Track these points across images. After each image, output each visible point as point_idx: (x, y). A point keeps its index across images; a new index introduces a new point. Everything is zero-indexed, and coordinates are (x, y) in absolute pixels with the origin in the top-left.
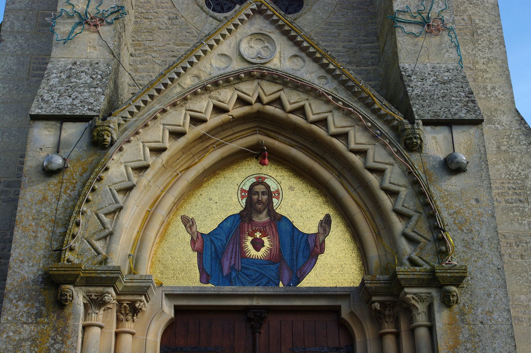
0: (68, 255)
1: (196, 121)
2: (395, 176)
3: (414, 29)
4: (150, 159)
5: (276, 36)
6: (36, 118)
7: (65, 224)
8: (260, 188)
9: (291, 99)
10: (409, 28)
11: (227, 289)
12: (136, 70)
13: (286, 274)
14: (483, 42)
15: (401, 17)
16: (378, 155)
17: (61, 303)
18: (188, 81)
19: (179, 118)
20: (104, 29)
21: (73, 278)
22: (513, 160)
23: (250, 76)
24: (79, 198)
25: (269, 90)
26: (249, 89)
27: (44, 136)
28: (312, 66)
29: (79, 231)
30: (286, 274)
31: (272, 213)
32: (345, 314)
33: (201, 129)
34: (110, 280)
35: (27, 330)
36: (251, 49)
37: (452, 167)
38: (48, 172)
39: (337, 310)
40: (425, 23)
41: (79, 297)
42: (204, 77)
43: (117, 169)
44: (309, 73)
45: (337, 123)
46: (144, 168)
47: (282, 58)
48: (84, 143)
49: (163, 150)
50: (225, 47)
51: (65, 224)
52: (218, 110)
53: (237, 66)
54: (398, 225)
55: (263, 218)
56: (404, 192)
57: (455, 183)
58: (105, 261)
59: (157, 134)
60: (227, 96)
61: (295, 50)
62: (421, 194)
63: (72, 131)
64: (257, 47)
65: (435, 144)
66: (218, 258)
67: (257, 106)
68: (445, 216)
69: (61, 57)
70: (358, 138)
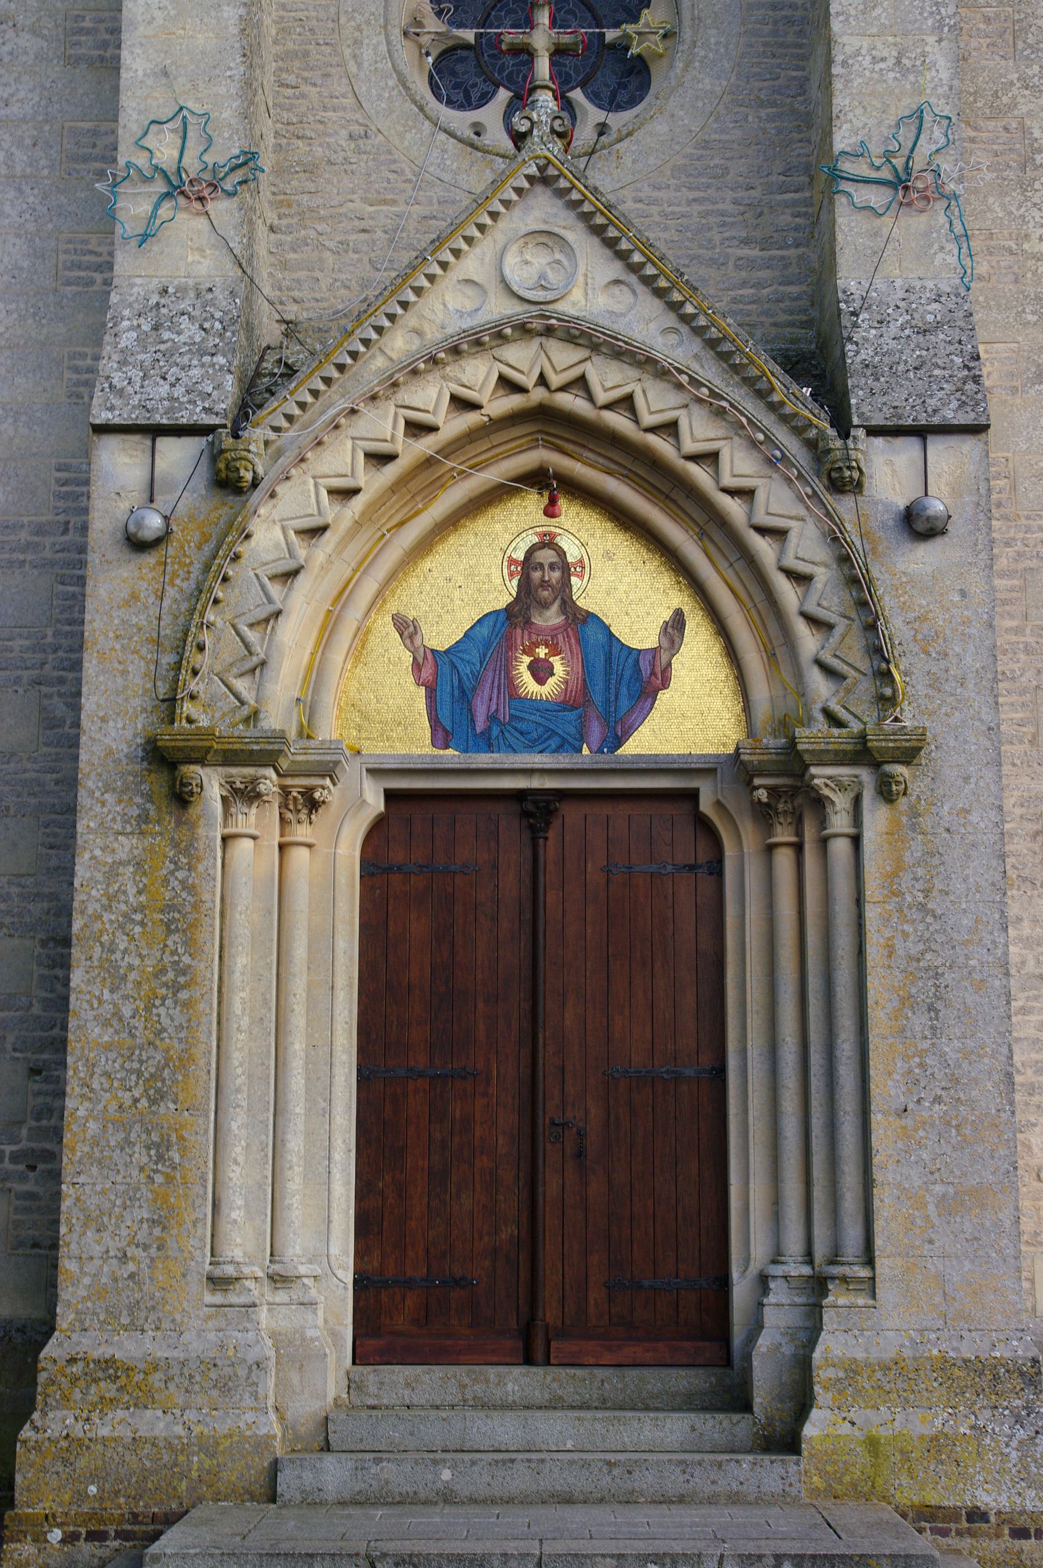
1: (417, 429)
2: (807, 546)
5: (576, 235)
7: (178, 652)
9: (608, 378)
11: (483, 759)
13: (596, 731)
16: (776, 501)
18: (400, 344)
19: (383, 425)
20: (220, 208)
23: (524, 330)
24: (201, 597)
25: (563, 359)
26: (522, 358)
27: (120, 465)
28: (650, 306)
30: (596, 731)
31: (568, 605)
33: (427, 445)
36: (526, 267)
37: (918, 525)
38: (137, 545)
42: (433, 335)
43: (268, 535)
44: (643, 322)
45: (699, 431)
46: (317, 532)
47: (592, 290)
50: (474, 264)
51: (178, 652)
52: (461, 404)
53: (499, 308)
54: (808, 641)
55: (551, 618)
56: (823, 576)
57: (922, 558)
59: (341, 459)
60: (477, 375)
61: (615, 269)
62: (856, 582)
63: (177, 456)
64: (539, 260)
65: (890, 473)
66: (464, 696)
67: (538, 395)
68: (896, 625)
69: (136, 276)
70: (739, 464)
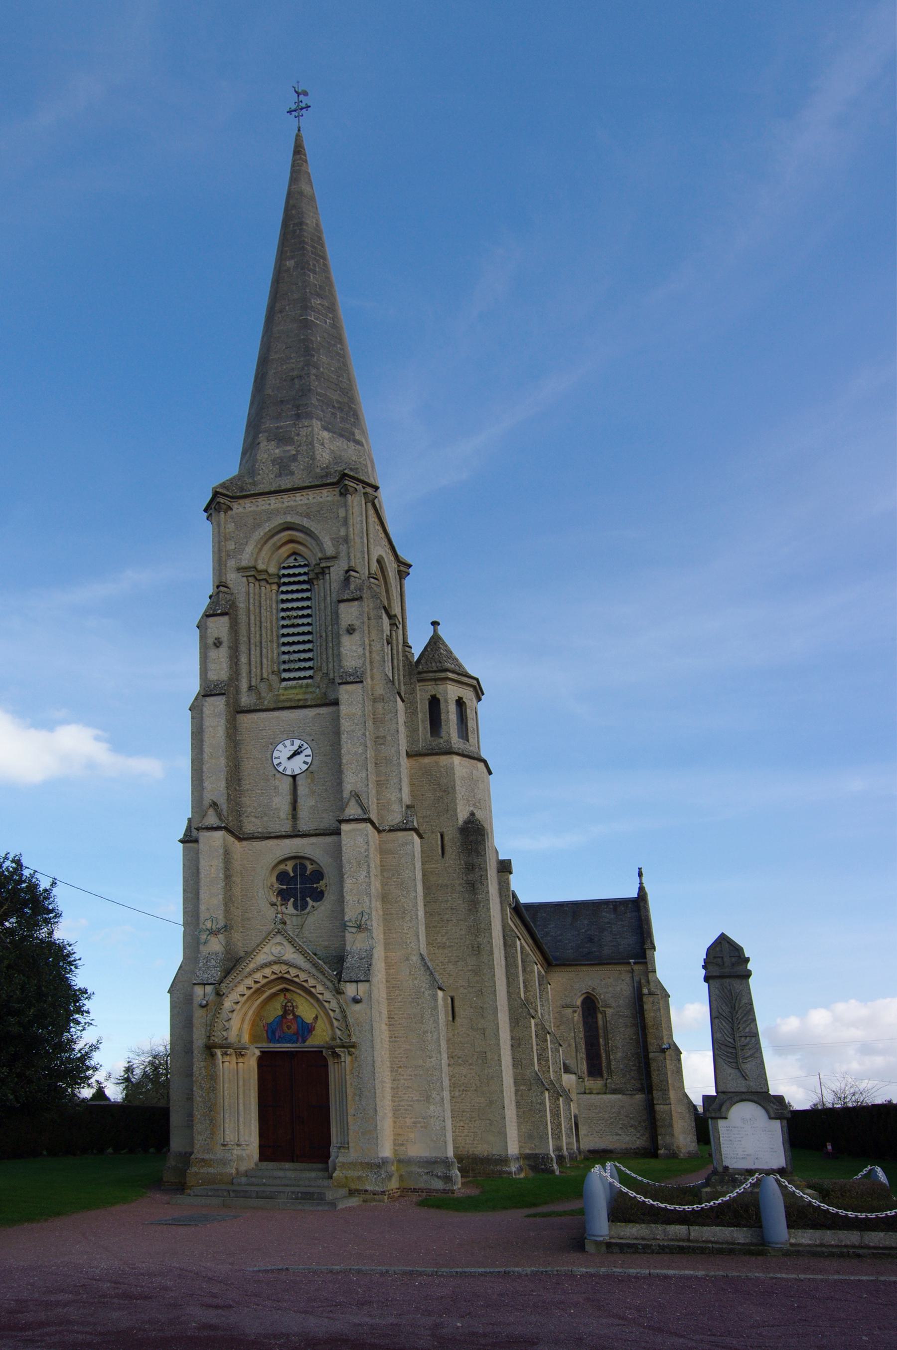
0: (212, 1038)
1: (256, 982)
2: (334, 1004)
3: (354, 930)
4: (235, 1006)
5: (286, 943)
6: (195, 984)
7: (210, 1027)
8: (289, 1004)
9: (293, 972)
10: (350, 930)
11: (278, 1045)
12: (245, 940)
13: (300, 1040)
14: (408, 918)
15: (348, 924)
16: (328, 995)
17: (213, 1055)
18: (252, 966)
19: (249, 982)
20: (221, 936)
21: (216, 1046)
22: (416, 979)
23: (275, 963)
24: (215, 1016)
25: (284, 968)
26: (276, 968)
27: (199, 991)
28: (301, 957)
29: (215, 1029)
30: (300, 1040)
31: (294, 1015)
32: (324, 1054)
33: (258, 985)
34: (228, 1047)
35: (203, 1064)
36: (276, 950)
37: (356, 1001)
38: (202, 1007)
39: (322, 1052)
40: (359, 927)
41: (219, 1052)
42: (258, 964)
43: (228, 1004)
44: (300, 960)
45: (312, 982)
46: (238, 1003)
47: (290, 954)
48: (214, 994)
49: (244, 995)
50: (266, 950)
51: (210, 1027)
52: (265, 977)
53: (272, 958)
54: (336, 1023)
55: (291, 1017)
56: (337, 1010)
57: (357, 1007)
58: (226, 1039)
59: (242, 989)
60: (267, 971)
61: (294, 950)
62: (343, 1011)
63: (209, 989)
64: (279, 948)
65: (350, 990)
66: (274, 1033)
67: (280, 975)
68: (350, 1020)
69: (204, 950)
70: (320, 988)
